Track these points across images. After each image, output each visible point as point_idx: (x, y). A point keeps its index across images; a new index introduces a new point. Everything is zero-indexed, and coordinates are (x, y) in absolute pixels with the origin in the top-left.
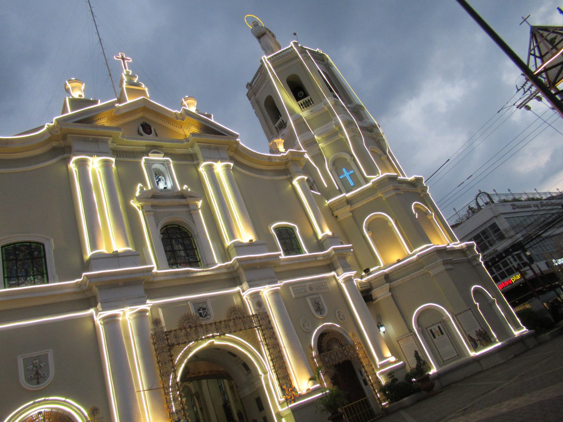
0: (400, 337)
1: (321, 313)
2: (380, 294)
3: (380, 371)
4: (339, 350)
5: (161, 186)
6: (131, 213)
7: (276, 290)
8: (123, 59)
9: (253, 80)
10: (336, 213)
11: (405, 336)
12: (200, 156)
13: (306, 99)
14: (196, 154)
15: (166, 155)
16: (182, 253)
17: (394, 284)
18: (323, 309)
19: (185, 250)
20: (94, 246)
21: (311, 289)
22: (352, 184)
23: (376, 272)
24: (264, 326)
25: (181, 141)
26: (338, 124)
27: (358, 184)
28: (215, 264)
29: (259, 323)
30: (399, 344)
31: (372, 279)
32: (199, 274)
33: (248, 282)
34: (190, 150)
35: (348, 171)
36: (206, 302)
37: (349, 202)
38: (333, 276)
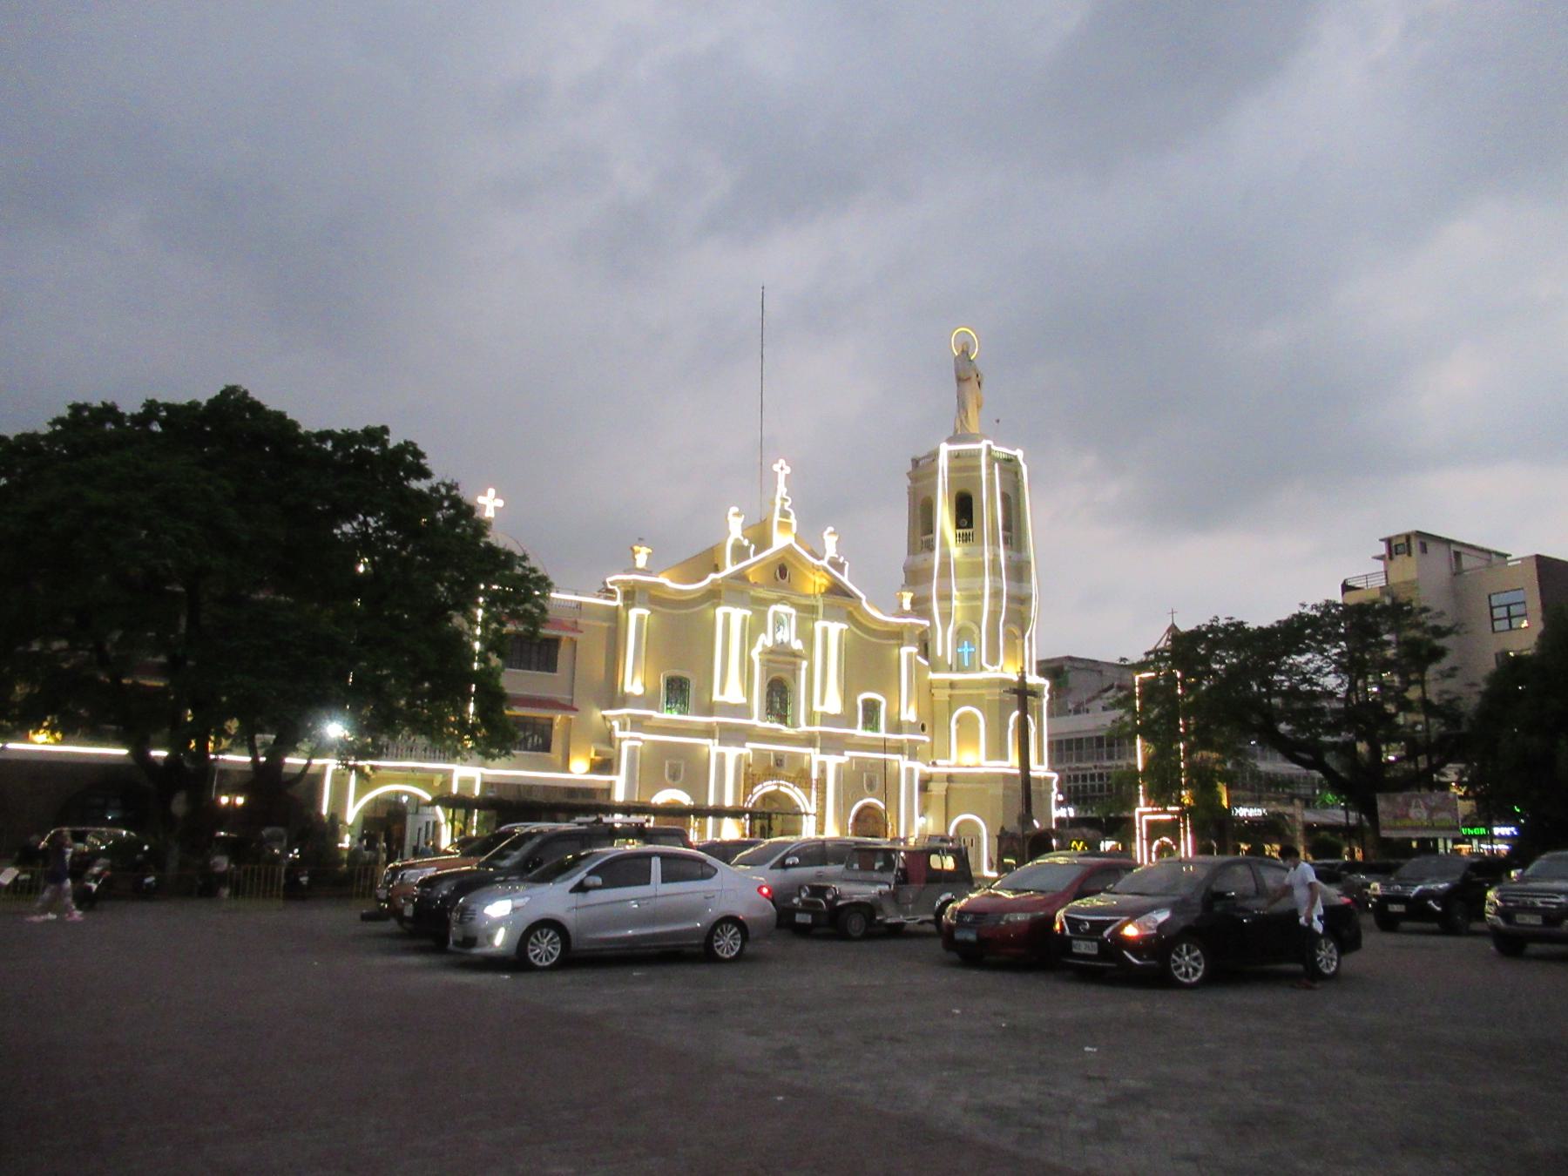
2: (937, 789)
5: (779, 637)
6: (751, 662)
8: (782, 469)
9: (924, 458)
10: (933, 691)
12: (821, 611)
13: (967, 531)
14: (817, 607)
15: (793, 605)
16: (778, 706)
19: (781, 703)
20: (722, 692)
22: (966, 664)
23: (944, 767)
25: (807, 596)
26: (982, 588)
27: (971, 669)
28: (799, 726)
33: (821, 748)
34: (814, 603)
35: (969, 647)
37: (952, 685)
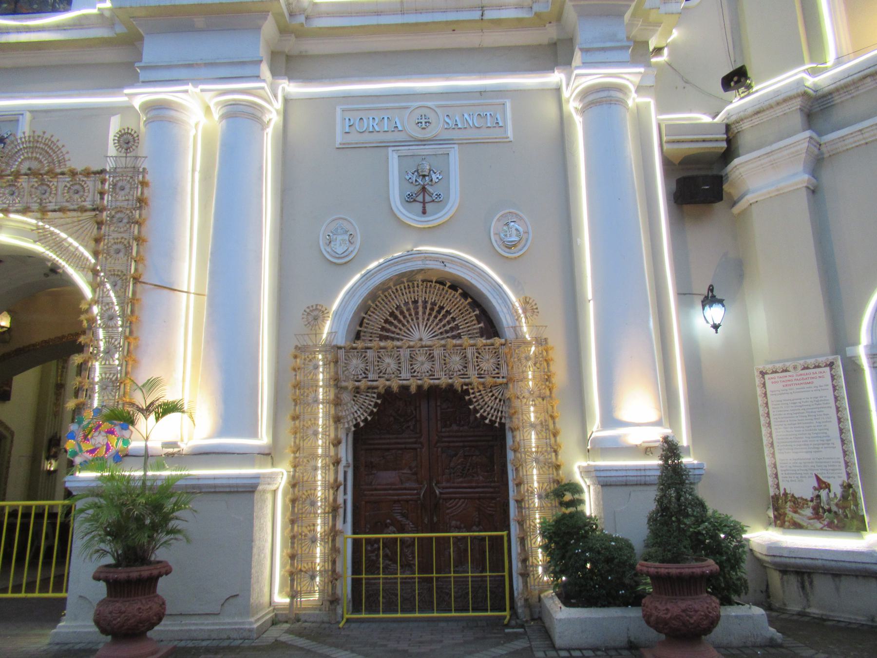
0: (779, 362)
1: (424, 207)
3: (584, 463)
4: (430, 346)
7: (235, 104)
11: (802, 362)
17: (842, 138)
18: (439, 195)
21: (424, 123)
24: (113, 213)
29: (102, 199)
30: (764, 385)
31: (742, 114)
32: (13, 38)
36: (18, 120)
38: (554, 87)
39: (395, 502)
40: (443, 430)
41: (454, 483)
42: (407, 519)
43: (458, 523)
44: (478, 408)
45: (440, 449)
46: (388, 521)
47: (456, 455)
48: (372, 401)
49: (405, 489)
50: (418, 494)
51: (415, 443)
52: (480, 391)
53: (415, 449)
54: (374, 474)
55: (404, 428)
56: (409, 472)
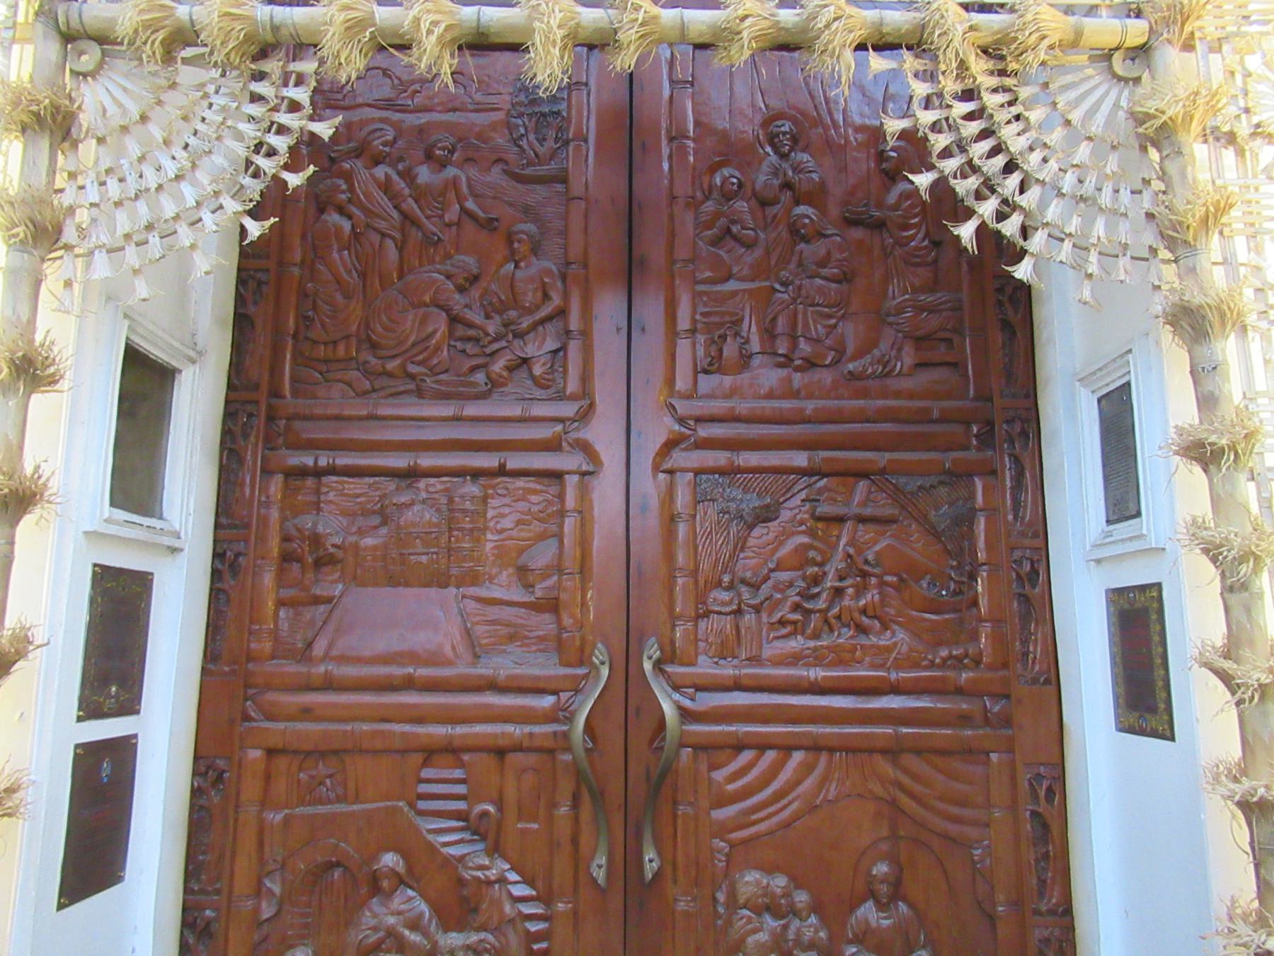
39: (432, 753)
40: (706, 383)
41: (755, 660)
42: (495, 849)
43: (780, 882)
44: (964, 187)
45: (684, 480)
46: (390, 859)
47: (766, 515)
48: (282, 130)
49: (492, 686)
50: (562, 715)
51: (552, 446)
52: (968, 95)
53: (557, 476)
54: (329, 600)
55: (498, 366)
56: (518, 595)
